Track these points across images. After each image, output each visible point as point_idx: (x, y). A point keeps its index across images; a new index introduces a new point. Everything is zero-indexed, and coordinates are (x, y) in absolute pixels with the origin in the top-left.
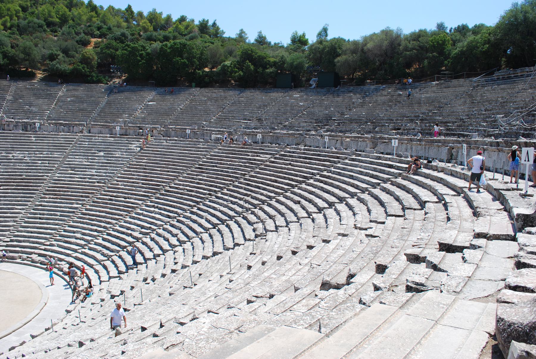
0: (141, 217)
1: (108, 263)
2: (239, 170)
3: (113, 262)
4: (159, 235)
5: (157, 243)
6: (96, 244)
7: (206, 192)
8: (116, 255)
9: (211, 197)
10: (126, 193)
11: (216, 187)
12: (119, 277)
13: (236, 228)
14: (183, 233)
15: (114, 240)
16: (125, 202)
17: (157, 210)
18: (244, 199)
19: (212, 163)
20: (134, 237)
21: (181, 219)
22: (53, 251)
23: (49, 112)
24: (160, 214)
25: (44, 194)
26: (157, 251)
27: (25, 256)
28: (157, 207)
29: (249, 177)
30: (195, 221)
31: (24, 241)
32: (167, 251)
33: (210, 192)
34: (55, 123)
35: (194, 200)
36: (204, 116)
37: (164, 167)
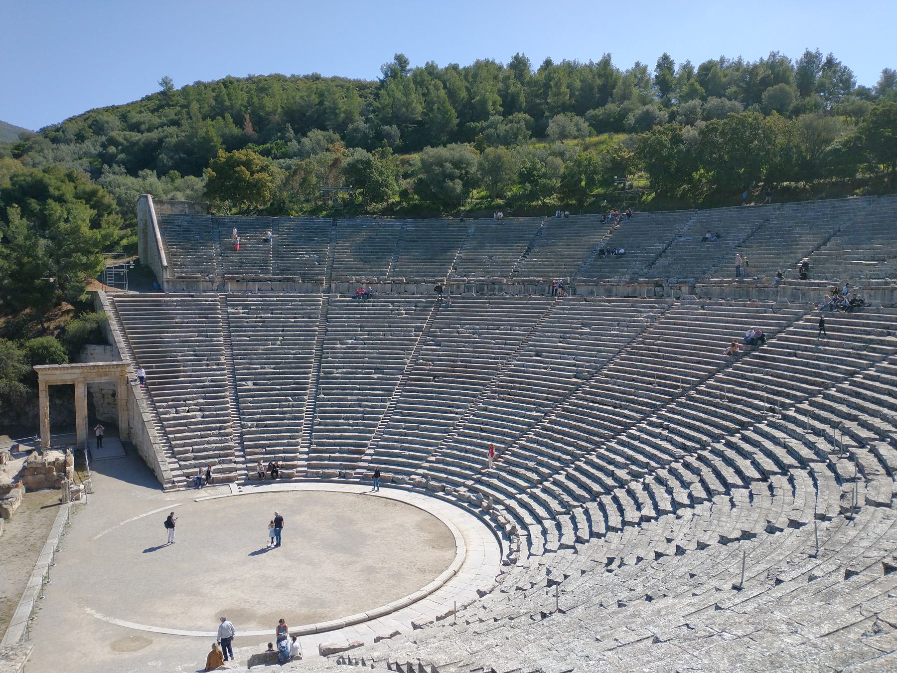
0: (637, 443)
1: (565, 519)
2: (843, 363)
3: (573, 519)
4: (660, 481)
5: (652, 496)
6: (555, 483)
7: (762, 404)
8: (581, 506)
9: (773, 416)
10: (618, 398)
11: (788, 396)
12: (573, 547)
13: (807, 486)
14: (702, 482)
15: (584, 479)
16: (614, 413)
17: (665, 433)
18: (841, 425)
19: (787, 347)
20: (616, 479)
21: (705, 453)
22: (490, 486)
23: (516, 264)
24: (671, 441)
25: (495, 392)
26: (648, 511)
27: (449, 487)
28: (667, 428)
29: (863, 378)
30: (729, 462)
31: (453, 465)
32: (666, 512)
33: (773, 406)
34: (523, 281)
35: (738, 420)
36: (784, 256)
37: (691, 355)
